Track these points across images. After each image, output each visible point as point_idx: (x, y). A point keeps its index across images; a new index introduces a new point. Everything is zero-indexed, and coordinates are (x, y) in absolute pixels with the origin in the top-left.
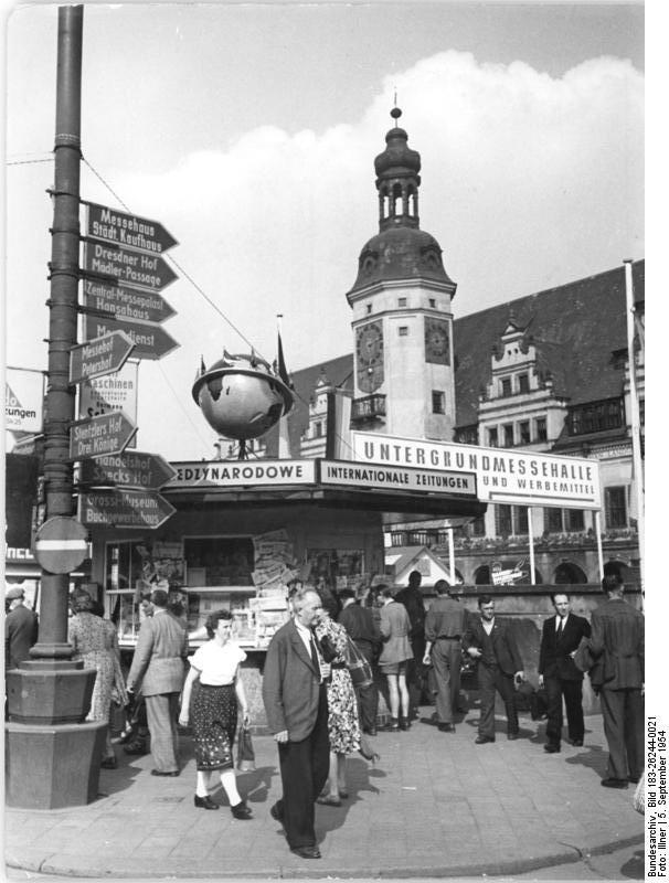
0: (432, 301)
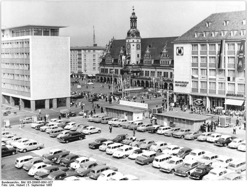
0: (138, 41)
